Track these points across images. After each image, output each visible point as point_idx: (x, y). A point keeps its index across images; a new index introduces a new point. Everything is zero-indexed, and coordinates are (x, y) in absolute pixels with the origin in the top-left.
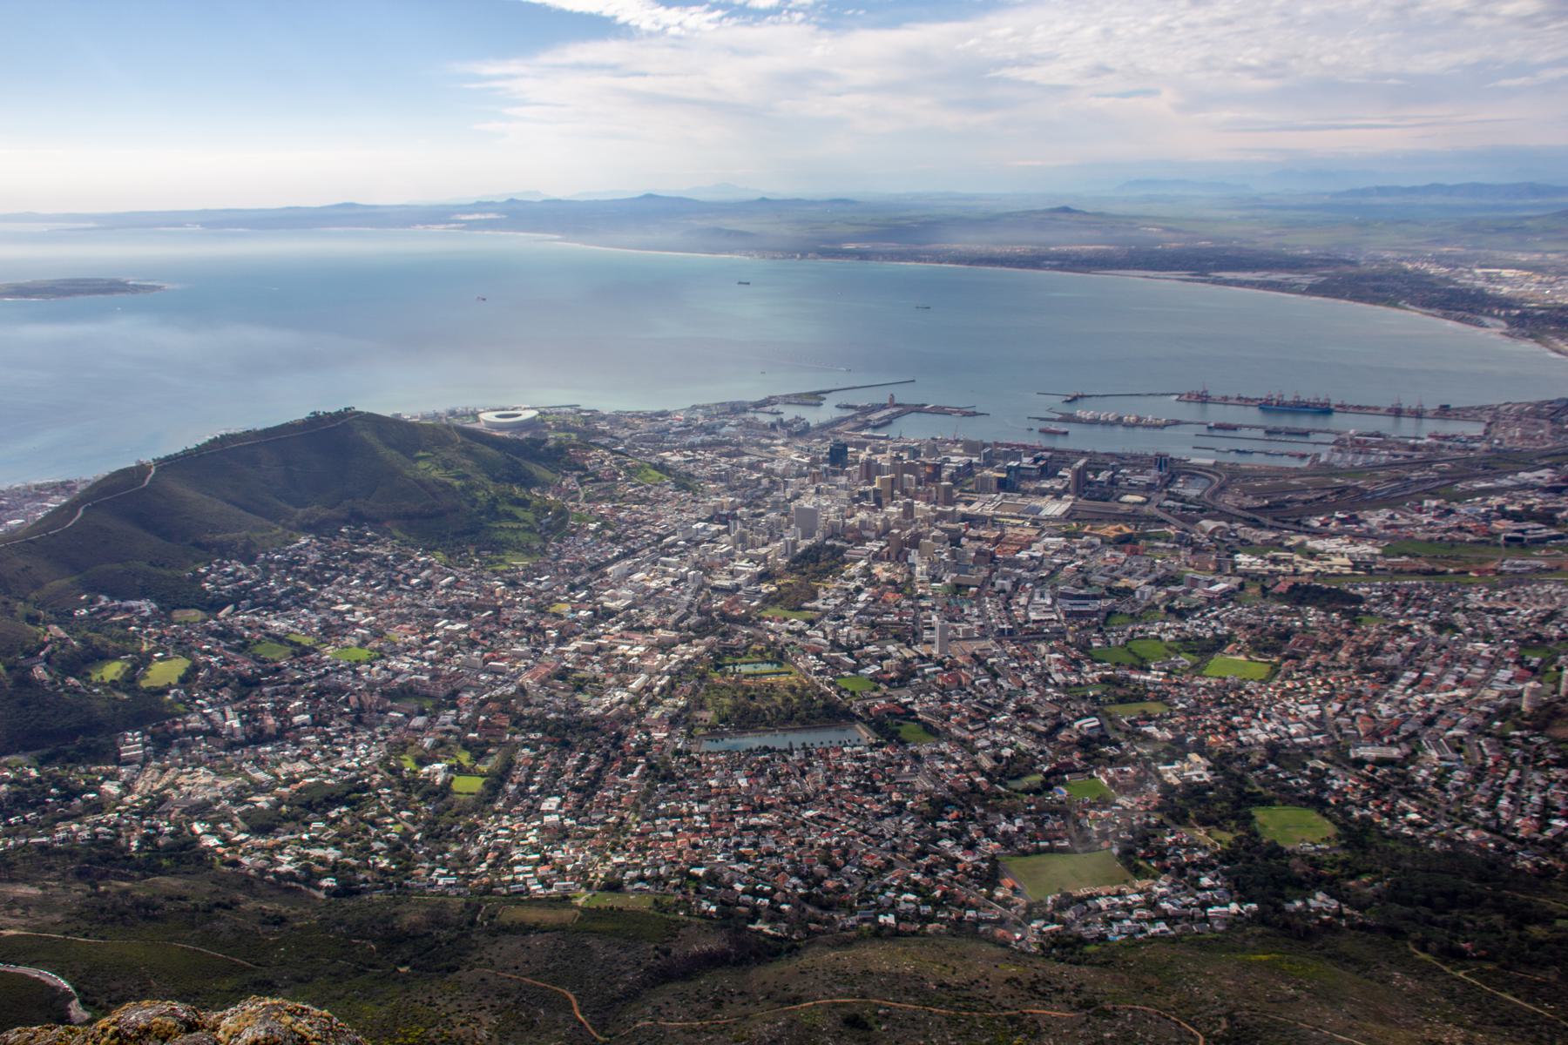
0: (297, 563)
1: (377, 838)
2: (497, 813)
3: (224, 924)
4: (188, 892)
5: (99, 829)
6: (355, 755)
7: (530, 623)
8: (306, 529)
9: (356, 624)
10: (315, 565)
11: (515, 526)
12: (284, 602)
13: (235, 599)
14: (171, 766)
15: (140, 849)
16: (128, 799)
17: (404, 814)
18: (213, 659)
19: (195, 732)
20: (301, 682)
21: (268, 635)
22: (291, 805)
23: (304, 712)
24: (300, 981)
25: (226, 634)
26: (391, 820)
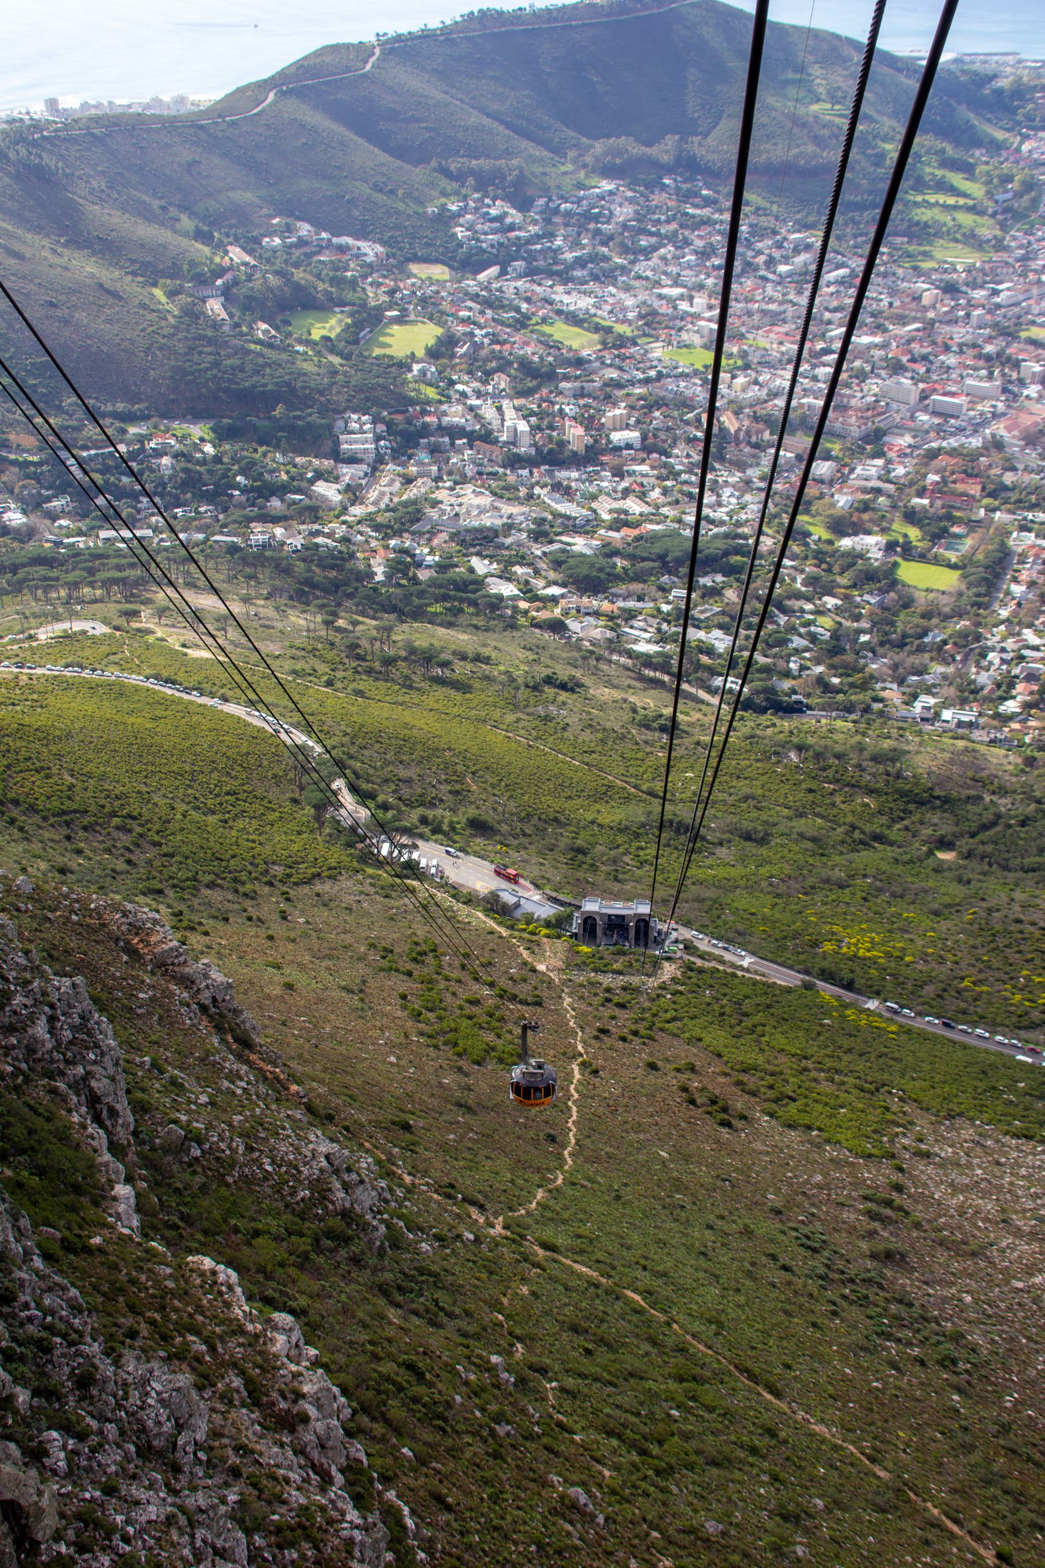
0: (596, 218)
1: (792, 629)
2: (1007, 621)
3: (567, 709)
4: (486, 651)
5: (320, 540)
6: (720, 504)
7: (989, 349)
8: (609, 172)
9: (697, 317)
10: (625, 226)
11: (951, 201)
12: (578, 273)
13: (503, 258)
14: (421, 475)
15: (389, 576)
16: (357, 511)
17: (830, 602)
18: (477, 332)
19: (454, 432)
20: (618, 385)
21: (559, 312)
22: (633, 558)
23: (627, 427)
24: (748, 837)
25: (492, 302)
26: (809, 607)
